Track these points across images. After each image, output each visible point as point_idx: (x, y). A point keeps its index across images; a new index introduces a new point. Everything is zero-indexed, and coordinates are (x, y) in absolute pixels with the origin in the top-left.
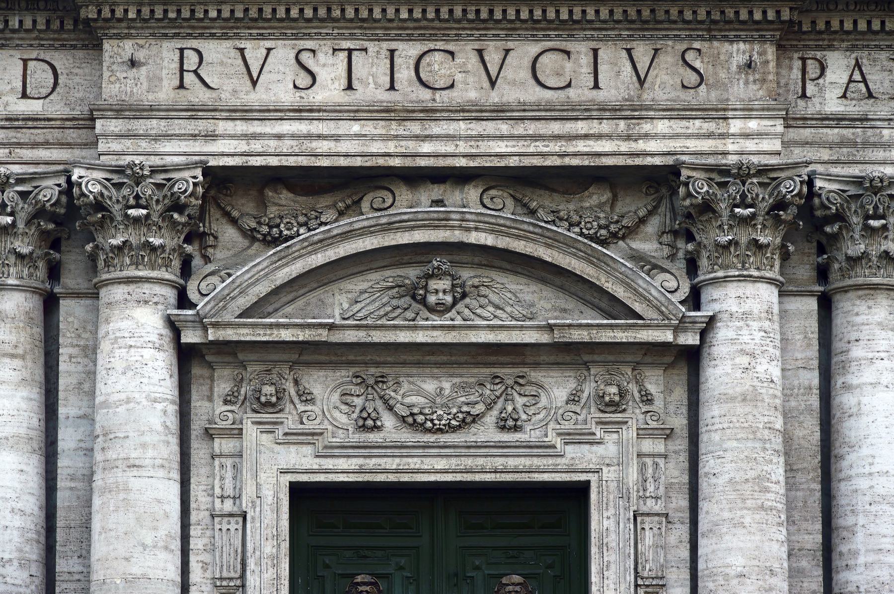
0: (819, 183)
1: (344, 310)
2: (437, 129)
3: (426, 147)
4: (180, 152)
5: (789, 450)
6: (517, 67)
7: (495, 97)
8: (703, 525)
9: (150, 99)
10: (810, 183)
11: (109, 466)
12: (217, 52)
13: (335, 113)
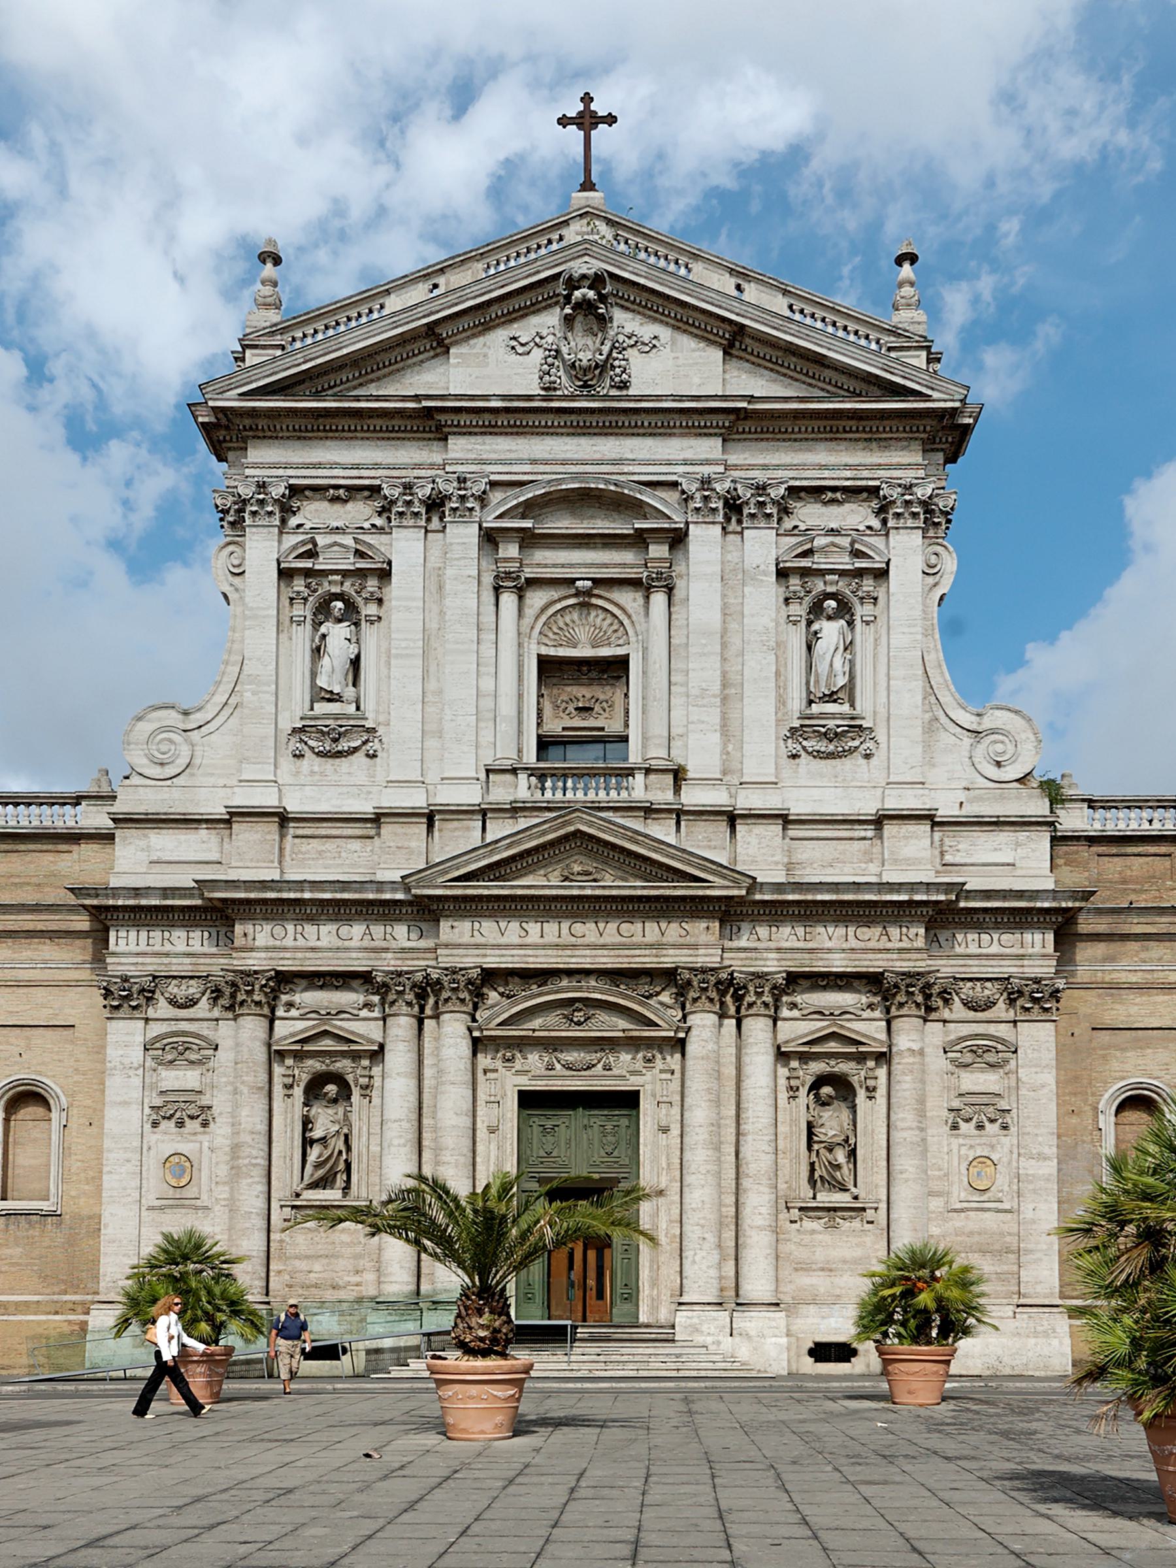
0: (735, 975)
2: (577, 953)
3: (573, 960)
7: (602, 941)
8: (686, 1106)
9: (460, 941)
10: (732, 974)
11: (443, 1083)
13: (535, 946)
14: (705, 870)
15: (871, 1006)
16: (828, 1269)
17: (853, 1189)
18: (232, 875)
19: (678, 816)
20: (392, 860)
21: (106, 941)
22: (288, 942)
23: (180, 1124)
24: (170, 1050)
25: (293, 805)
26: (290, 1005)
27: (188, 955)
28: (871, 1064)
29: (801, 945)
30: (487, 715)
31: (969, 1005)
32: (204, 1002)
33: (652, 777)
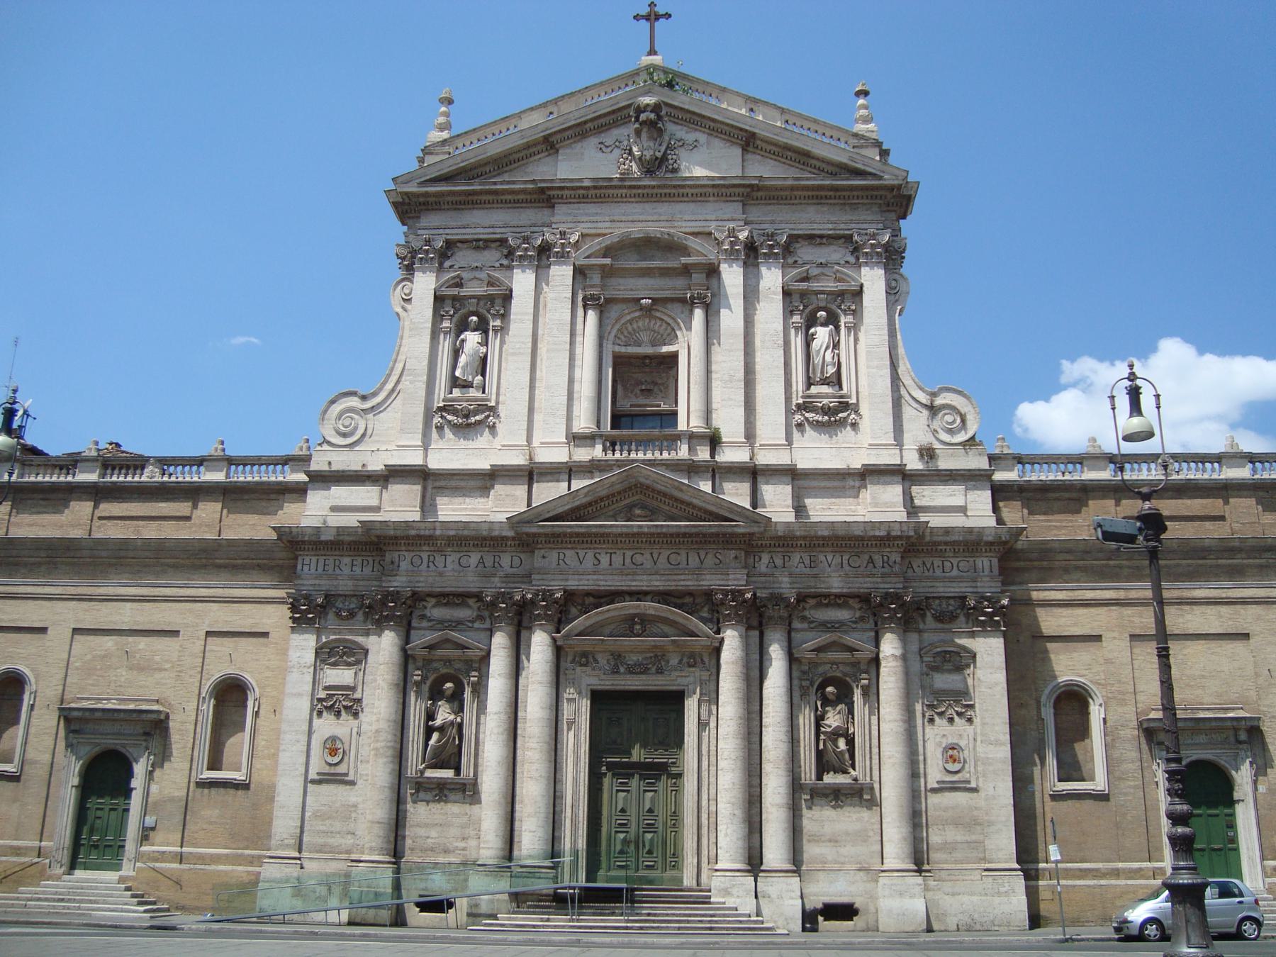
4: (557, 587)
6: (663, 559)
15: (862, 619)
16: (834, 841)
17: (853, 773)
19: (713, 470)
26: (423, 617)
31: (939, 618)
32: (360, 616)
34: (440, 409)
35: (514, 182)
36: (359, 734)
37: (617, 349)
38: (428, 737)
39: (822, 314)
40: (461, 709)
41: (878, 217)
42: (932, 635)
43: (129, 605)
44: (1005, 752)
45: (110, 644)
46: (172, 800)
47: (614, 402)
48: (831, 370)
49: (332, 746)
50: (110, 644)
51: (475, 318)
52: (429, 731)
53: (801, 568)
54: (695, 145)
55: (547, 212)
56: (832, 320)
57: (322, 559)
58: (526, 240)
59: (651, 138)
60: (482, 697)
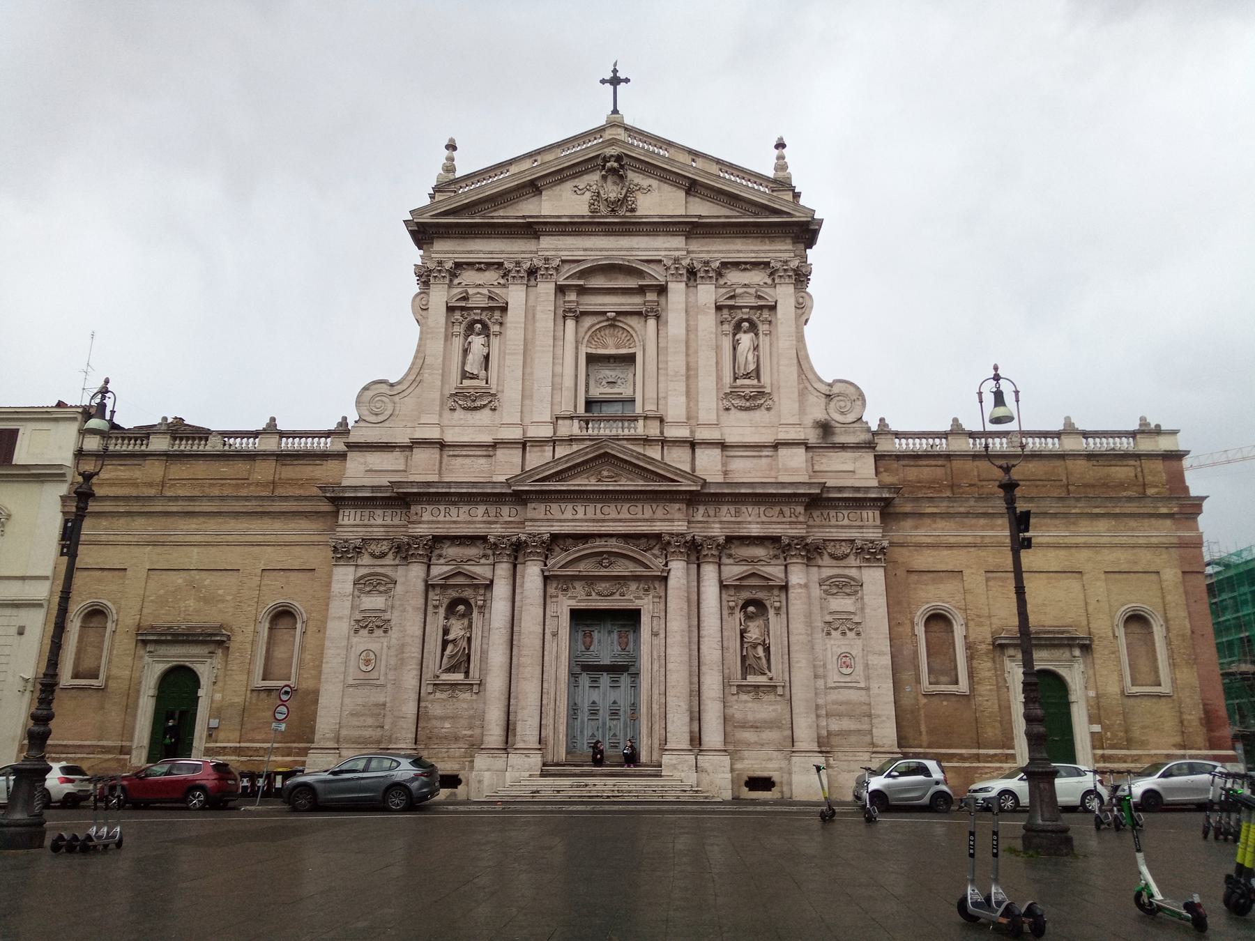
1: (584, 568)
4: (545, 530)
5: (689, 601)
7: (619, 517)
12: (555, 506)
14: (677, 474)
15: (776, 557)
16: (755, 727)
18: (411, 478)
20: (504, 468)
21: (337, 517)
22: (441, 518)
23: (371, 632)
24: (366, 584)
25: (449, 438)
26: (440, 556)
27: (383, 526)
28: (776, 592)
29: (733, 519)
30: (556, 387)
31: (832, 556)
32: (390, 555)
33: (649, 422)
34: (452, 395)
35: (507, 217)
36: (389, 648)
37: (590, 351)
38: (444, 649)
39: (746, 324)
40: (470, 626)
41: (790, 247)
42: (828, 569)
43: (196, 550)
44: (887, 661)
45: (180, 581)
46: (232, 705)
47: (587, 391)
48: (752, 367)
49: (368, 659)
50: (180, 581)
51: (479, 326)
52: (445, 644)
53: (728, 518)
54: (649, 190)
55: (534, 242)
56: (753, 328)
57: (359, 511)
58: (518, 263)
59: (615, 183)
60: (487, 616)
